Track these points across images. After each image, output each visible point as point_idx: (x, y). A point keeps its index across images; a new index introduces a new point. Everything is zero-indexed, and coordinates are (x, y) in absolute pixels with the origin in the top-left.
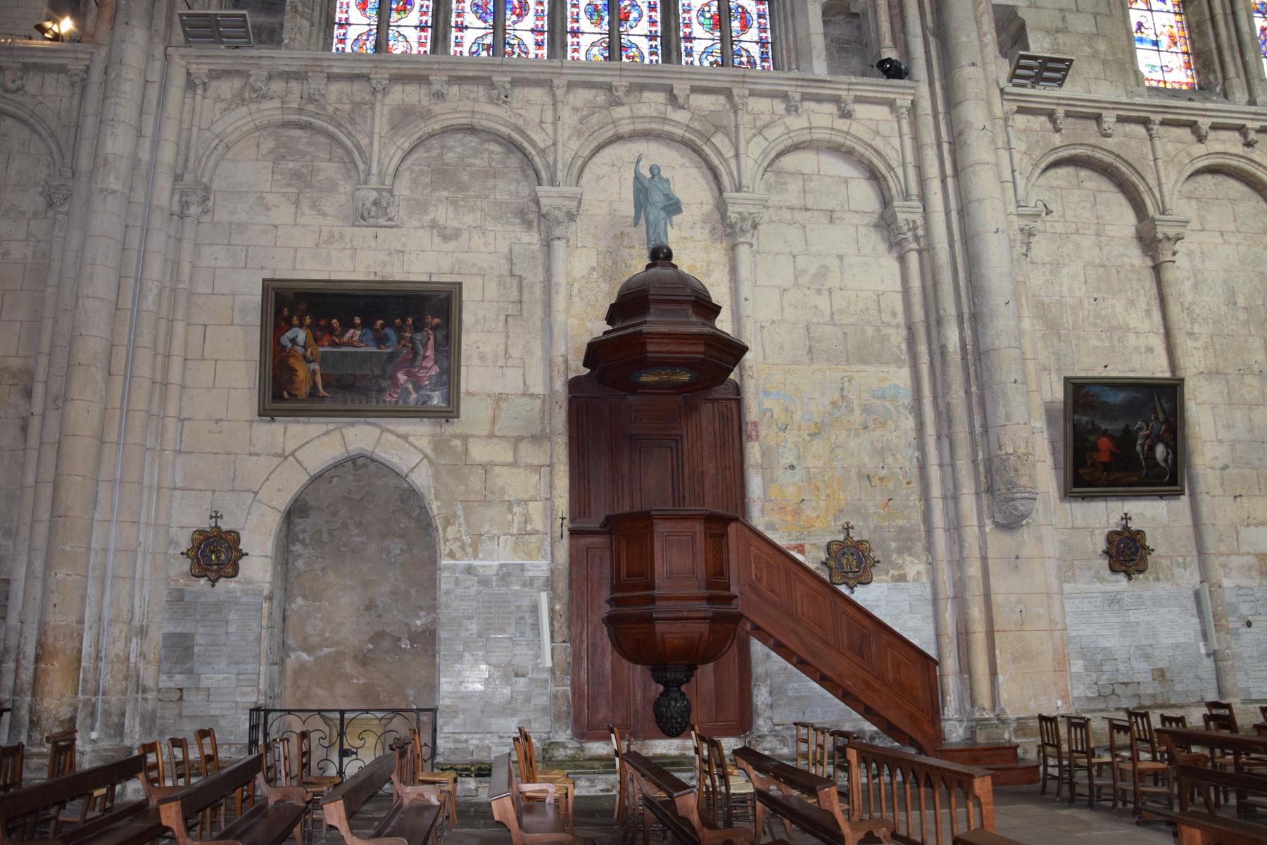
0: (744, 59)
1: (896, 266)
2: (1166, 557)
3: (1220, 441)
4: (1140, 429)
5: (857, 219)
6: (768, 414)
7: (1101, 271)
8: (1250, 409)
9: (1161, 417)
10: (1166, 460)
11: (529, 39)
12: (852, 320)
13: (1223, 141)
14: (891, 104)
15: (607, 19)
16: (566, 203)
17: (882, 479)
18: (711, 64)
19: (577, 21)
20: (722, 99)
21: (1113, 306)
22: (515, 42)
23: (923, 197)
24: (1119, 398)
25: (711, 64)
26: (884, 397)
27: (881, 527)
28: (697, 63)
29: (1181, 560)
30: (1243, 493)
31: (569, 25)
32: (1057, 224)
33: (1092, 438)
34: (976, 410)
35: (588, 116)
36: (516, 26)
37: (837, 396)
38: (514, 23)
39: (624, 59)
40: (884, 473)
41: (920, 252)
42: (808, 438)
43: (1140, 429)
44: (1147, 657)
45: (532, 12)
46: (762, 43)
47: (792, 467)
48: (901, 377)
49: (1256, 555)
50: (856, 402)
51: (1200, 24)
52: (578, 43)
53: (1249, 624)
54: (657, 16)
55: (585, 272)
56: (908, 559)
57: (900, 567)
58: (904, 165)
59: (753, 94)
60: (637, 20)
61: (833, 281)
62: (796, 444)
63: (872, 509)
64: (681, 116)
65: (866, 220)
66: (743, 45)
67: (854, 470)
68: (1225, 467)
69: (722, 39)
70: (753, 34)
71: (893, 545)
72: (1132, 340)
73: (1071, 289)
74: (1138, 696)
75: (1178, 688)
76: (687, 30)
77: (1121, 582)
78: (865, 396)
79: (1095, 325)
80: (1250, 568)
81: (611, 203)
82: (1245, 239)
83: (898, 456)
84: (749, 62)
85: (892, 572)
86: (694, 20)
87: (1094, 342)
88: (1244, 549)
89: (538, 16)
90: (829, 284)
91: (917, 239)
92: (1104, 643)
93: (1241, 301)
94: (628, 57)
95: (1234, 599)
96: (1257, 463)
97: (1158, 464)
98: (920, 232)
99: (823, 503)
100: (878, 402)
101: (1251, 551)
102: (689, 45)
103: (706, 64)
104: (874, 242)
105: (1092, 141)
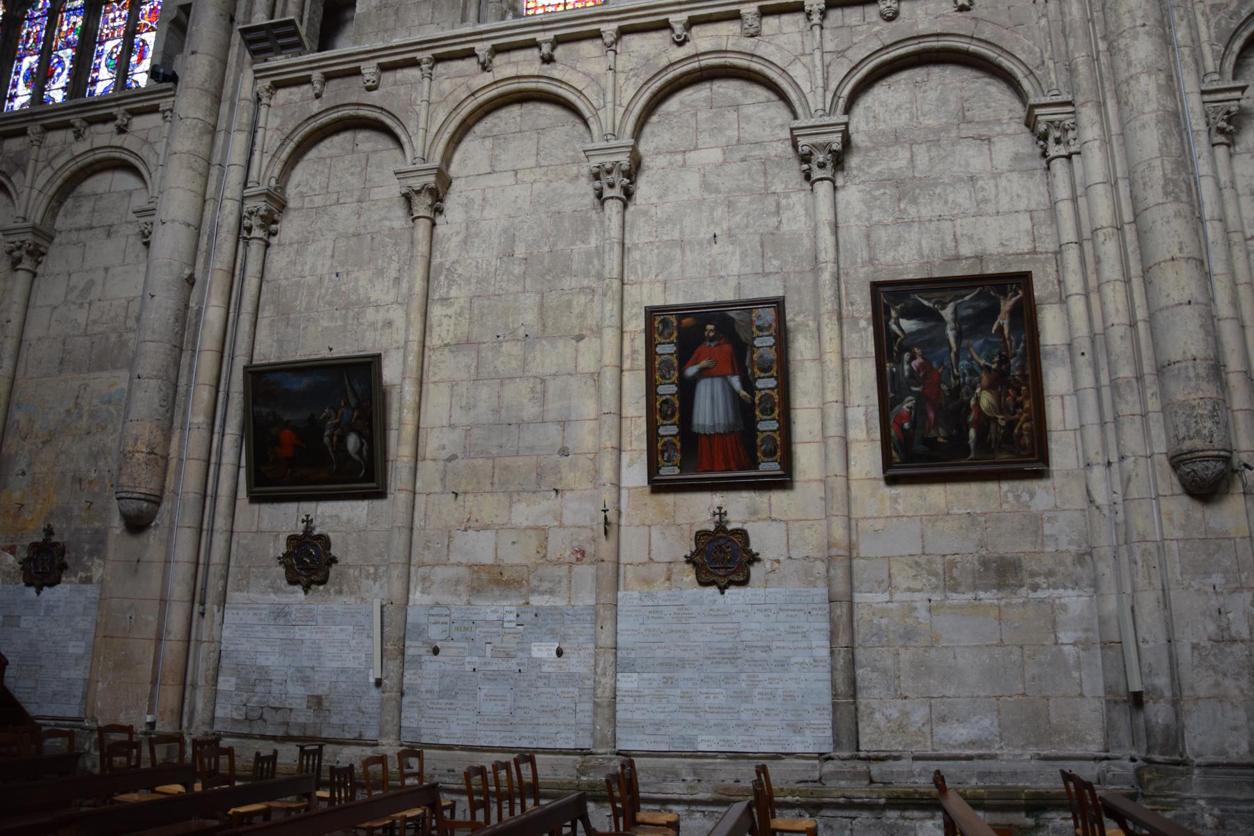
2: (354, 567)
3: (452, 426)
4: (328, 418)
7: (353, 241)
8: (502, 385)
9: (353, 402)
10: (360, 452)
13: (516, 64)
17: (90, 482)
21: (357, 279)
24: (303, 383)
26: (110, 402)
29: (372, 570)
30: (469, 488)
32: (316, 199)
37: (71, 404)
40: (93, 475)
42: (40, 445)
43: (328, 418)
44: (306, 681)
47: (24, 473)
49: (470, 567)
50: (86, 408)
53: (436, 651)
56: (97, 561)
57: (88, 569)
61: (95, 293)
63: (76, 512)
68: (453, 457)
71: (87, 547)
72: (370, 315)
73: (313, 268)
74: (287, 724)
75: (335, 720)
78: (95, 402)
79: (330, 303)
80: (457, 582)
82: (546, 174)
83: (109, 459)
85: (81, 574)
87: (325, 323)
90: (91, 297)
92: (262, 661)
93: (520, 251)
95: (423, 620)
96: (495, 452)
97: (349, 457)
100: (104, 407)
101: (464, 561)
105: (354, 99)
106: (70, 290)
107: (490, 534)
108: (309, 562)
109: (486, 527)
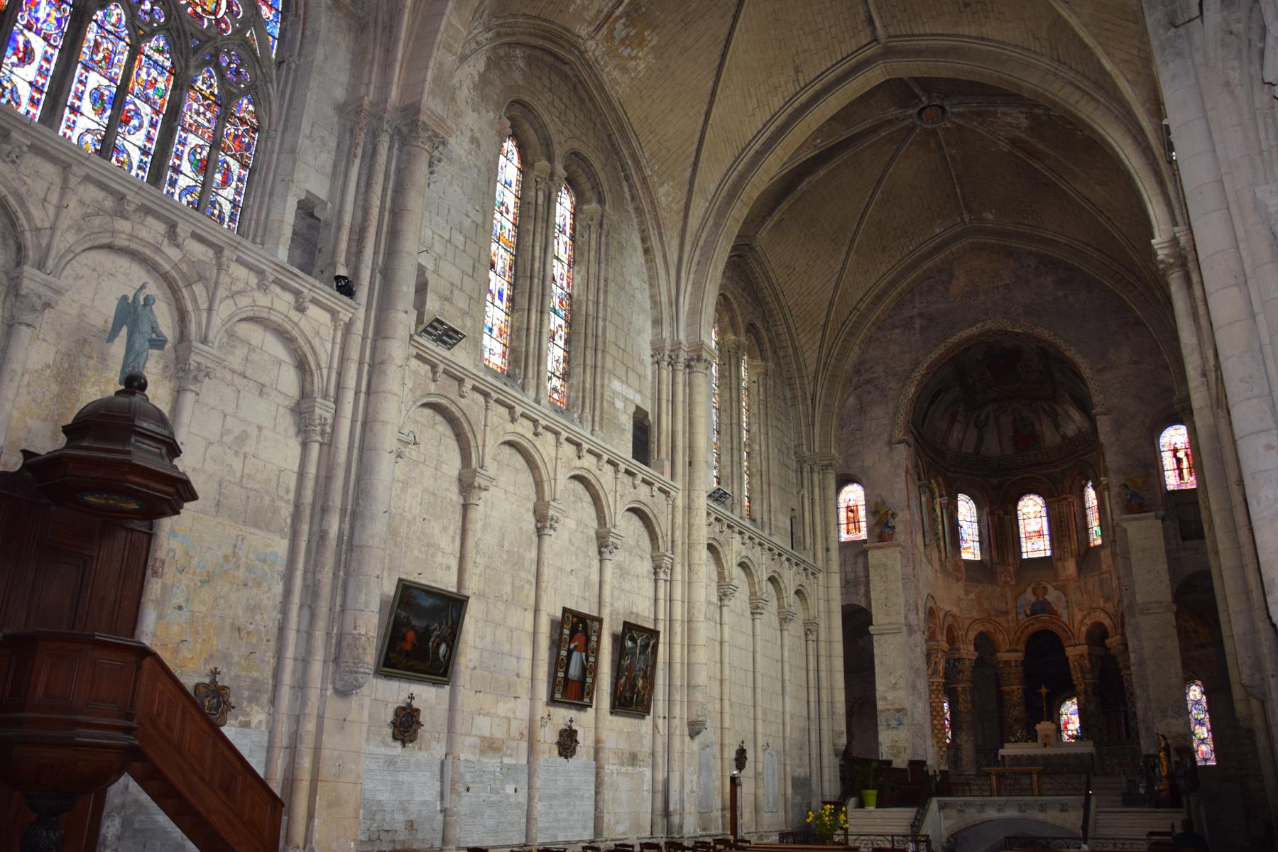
0: (216, 212)
1: (297, 450)
3: (475, 648)
5: (280, 399)
6: (171, 554)
7: (432, 498)
11: (25, 92)
12: (256, 487)
14: (334, 314)
15: (109, 112)
16: (49, 293)
17: (249, 633)
18: (189, 203)
19: (80, 99)
20: (211, 253)
22: (9, 85)
23: (337, 401)
24: (427, 602)
25: (189, 203)
26: (265, 561)
27: (239, 676)
28: (176, 197)
31: (70, 99)
33: (404, 630)
34: (339, 591)
35: (90, 215)
36: (15, 69)
37: (230, 551)
38: (13, 64)
39: (114, 160)
41: (321, 444)
44: (405, 810)
45: (35, 65)
46: (234, 204)
47: (180, 608)
48: (281, 547)
50: (243, 560)
51: (519, 329)
52: (74, 122)
53: (468, 789)
54: (155, 134)
55: (39, 367)
56: (256, 708)
57: (247, 714)
58: (330, 368)
59: (240, 261)
60: (138, 129)
61: (249, 448)
62: (188, 587)
63: (236, 659)
64: (174, 253)
65: (286, 403)
66: (219, 198)
67: (229, 621)
68: (474, 668)
69: (203, 184)
70: (229, 192)
71: (246, 694)
72: (439, 558)
74: (394, 841)
75: (419, 836)
76: (177, 162)
77: (397, 748)
78: (252, 556)
79: (419, 539)
80: (475, 747)
81: (82, 306)
84: (219, 216)
85: (241, 718)
86: (185, 156)
87: (416, 553)
88: (475, 732)
89: (40, 71)
90: (245, 449)
91: (323, 433)
92: (380, 797)
93: (506, 548)
94: (118, 160)
98: (328, 430)
99: (199, 646)
100: (260, 564)
102: (175, 176)
103: (184, 202)
104: (287, 423)
105: (453, 397)
106: (225, 432)
107: (487, 719)
108: (406, 725)
109: (487, 714)
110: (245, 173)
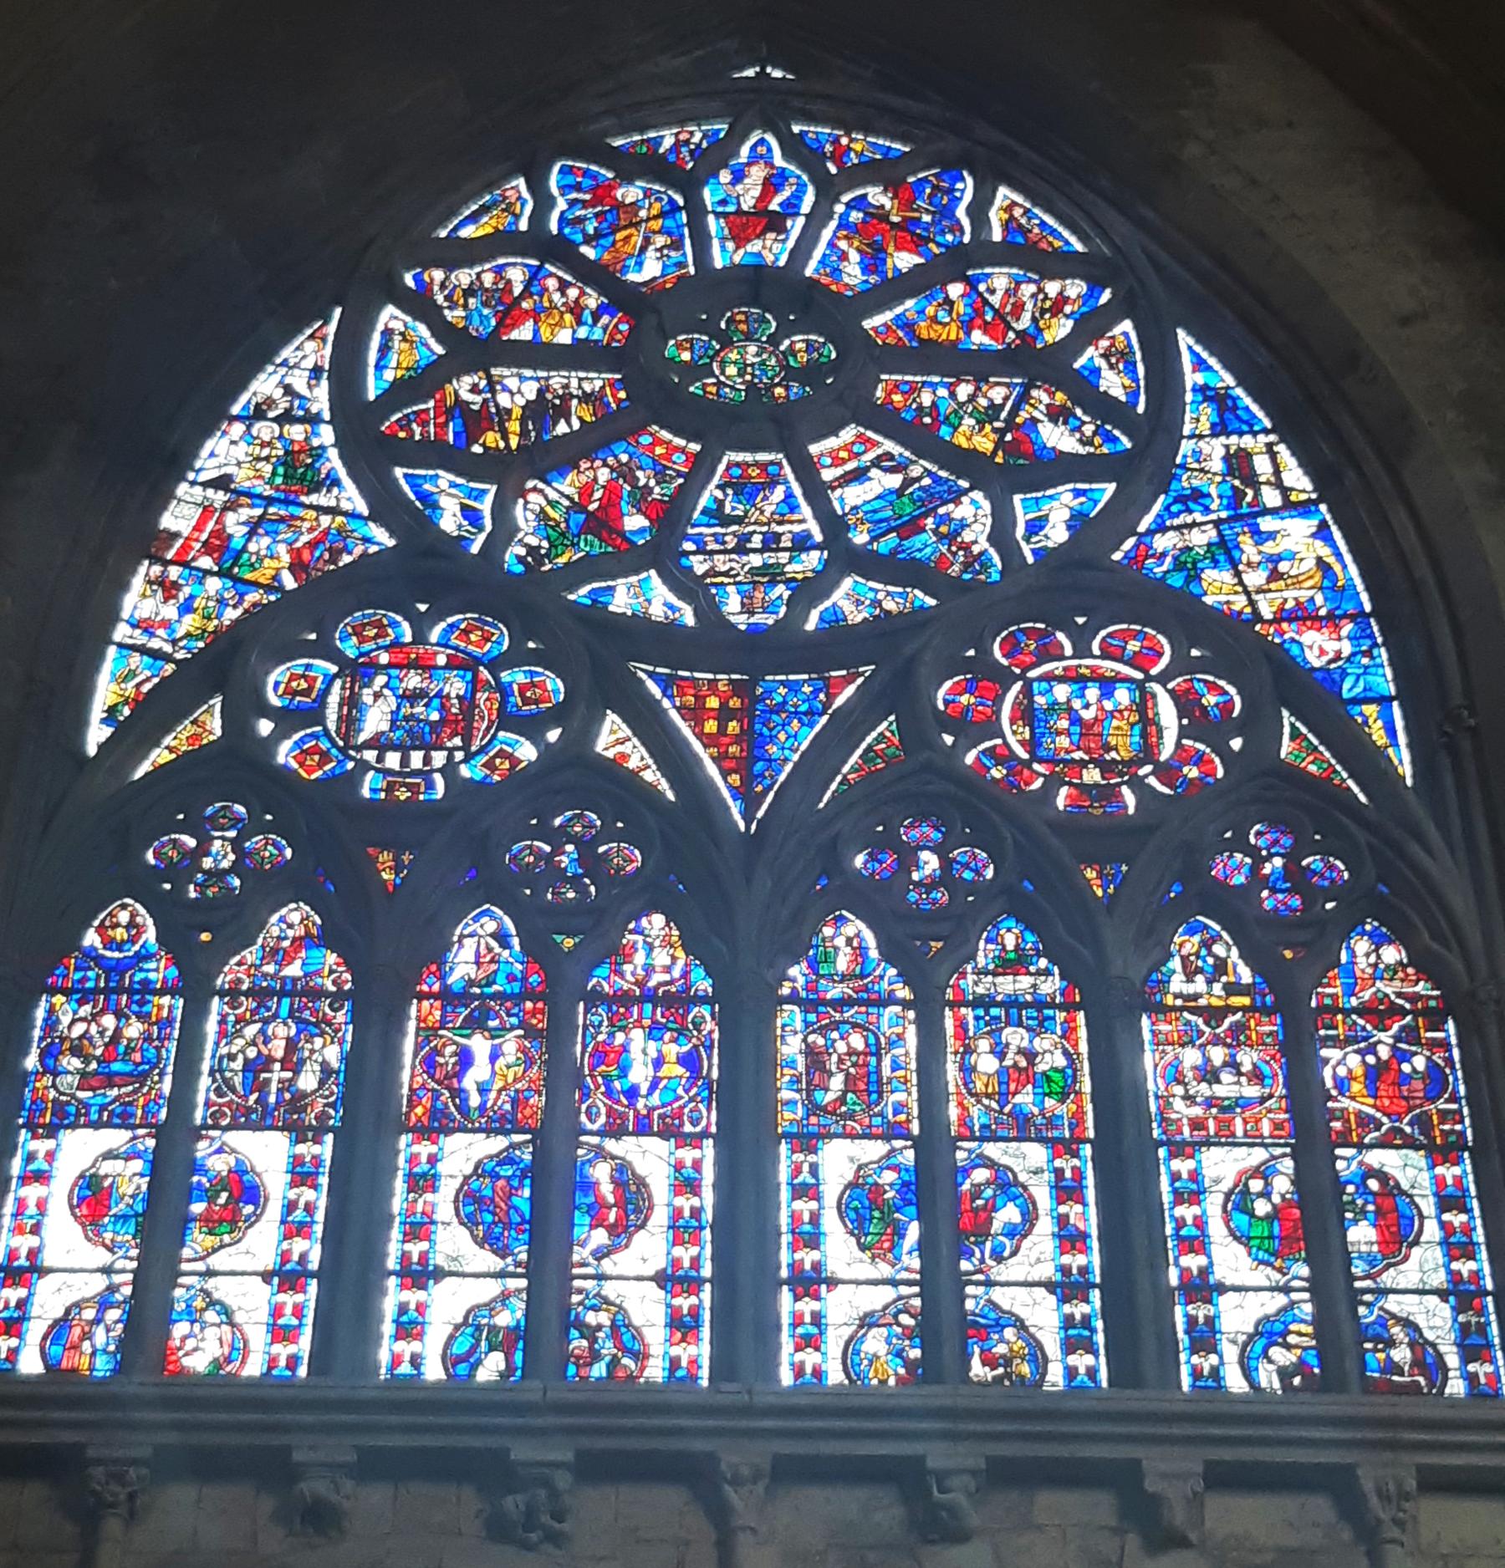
0: (1401, 1354)
11: (648, 1309)
15: (913, 1232)
18: (1284, 1374)
19: (813, 1241)
20: (1320, 1507)
22: (604, 1318)
25: (1284, 1374)
28: (1235, 1381)
31: (785, 1257)
36: (607, 1266)
38: (600, 1254)
39: (978, 1369)
45: (660, 1217)
46: (1460, 1293)
52: (817, 1319)
54: (1087, 1216)
60: (1019, 1233)
66: (1392, 1303)
69: (1315, 1287)
70: (1425, 1263)
76: (1193, 1262)
84: (1418, 1363)
86: (1216, 1228)
89: (681, 1231)
94: (989, 1361)
102: (1201, 1312)
103: (1267, 1377)
110: (1459, 1172)
